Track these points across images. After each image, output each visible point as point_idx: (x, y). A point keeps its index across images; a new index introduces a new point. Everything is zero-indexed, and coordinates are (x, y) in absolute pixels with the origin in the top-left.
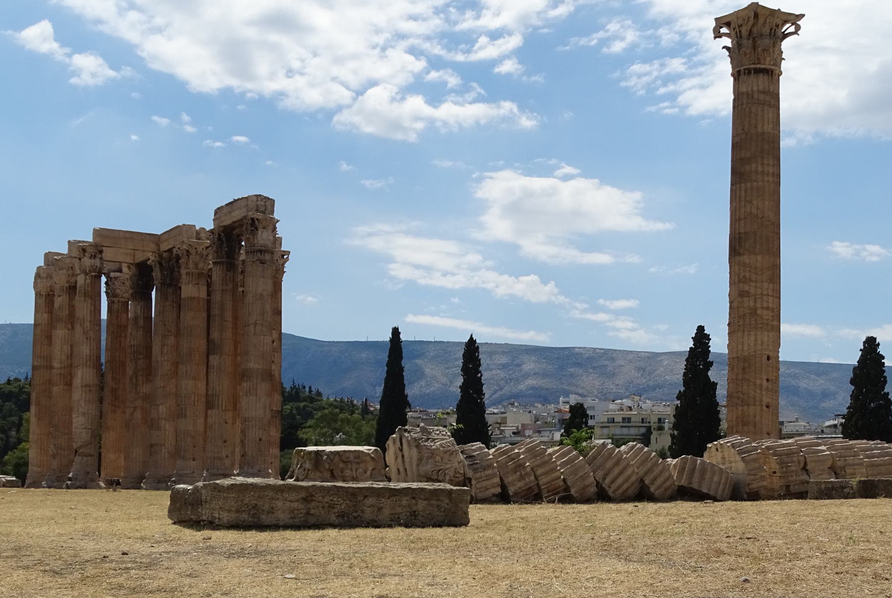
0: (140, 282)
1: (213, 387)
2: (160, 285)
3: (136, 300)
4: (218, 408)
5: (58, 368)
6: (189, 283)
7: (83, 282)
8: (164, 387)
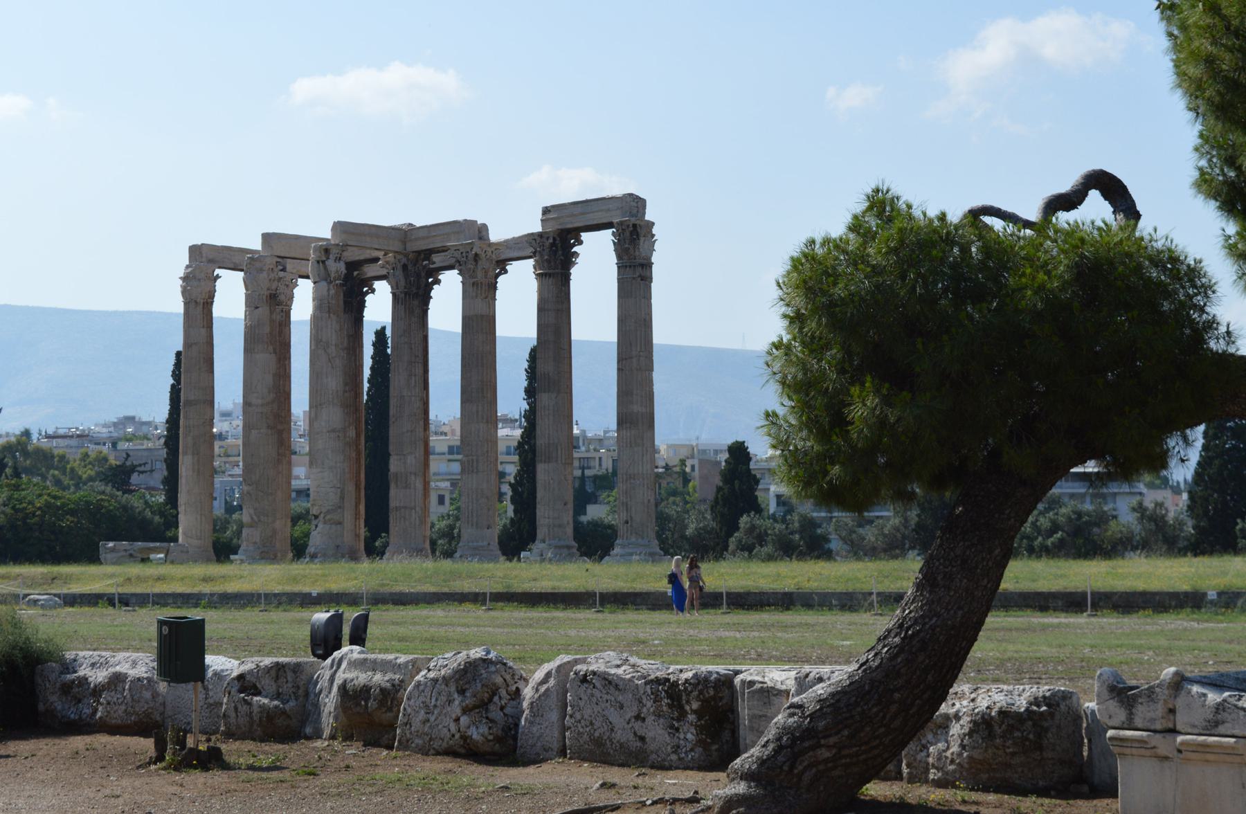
1: (549, 434)
4: (557, 461)
6: (476, 297)
7: (325, 293)
8: (412, 431)
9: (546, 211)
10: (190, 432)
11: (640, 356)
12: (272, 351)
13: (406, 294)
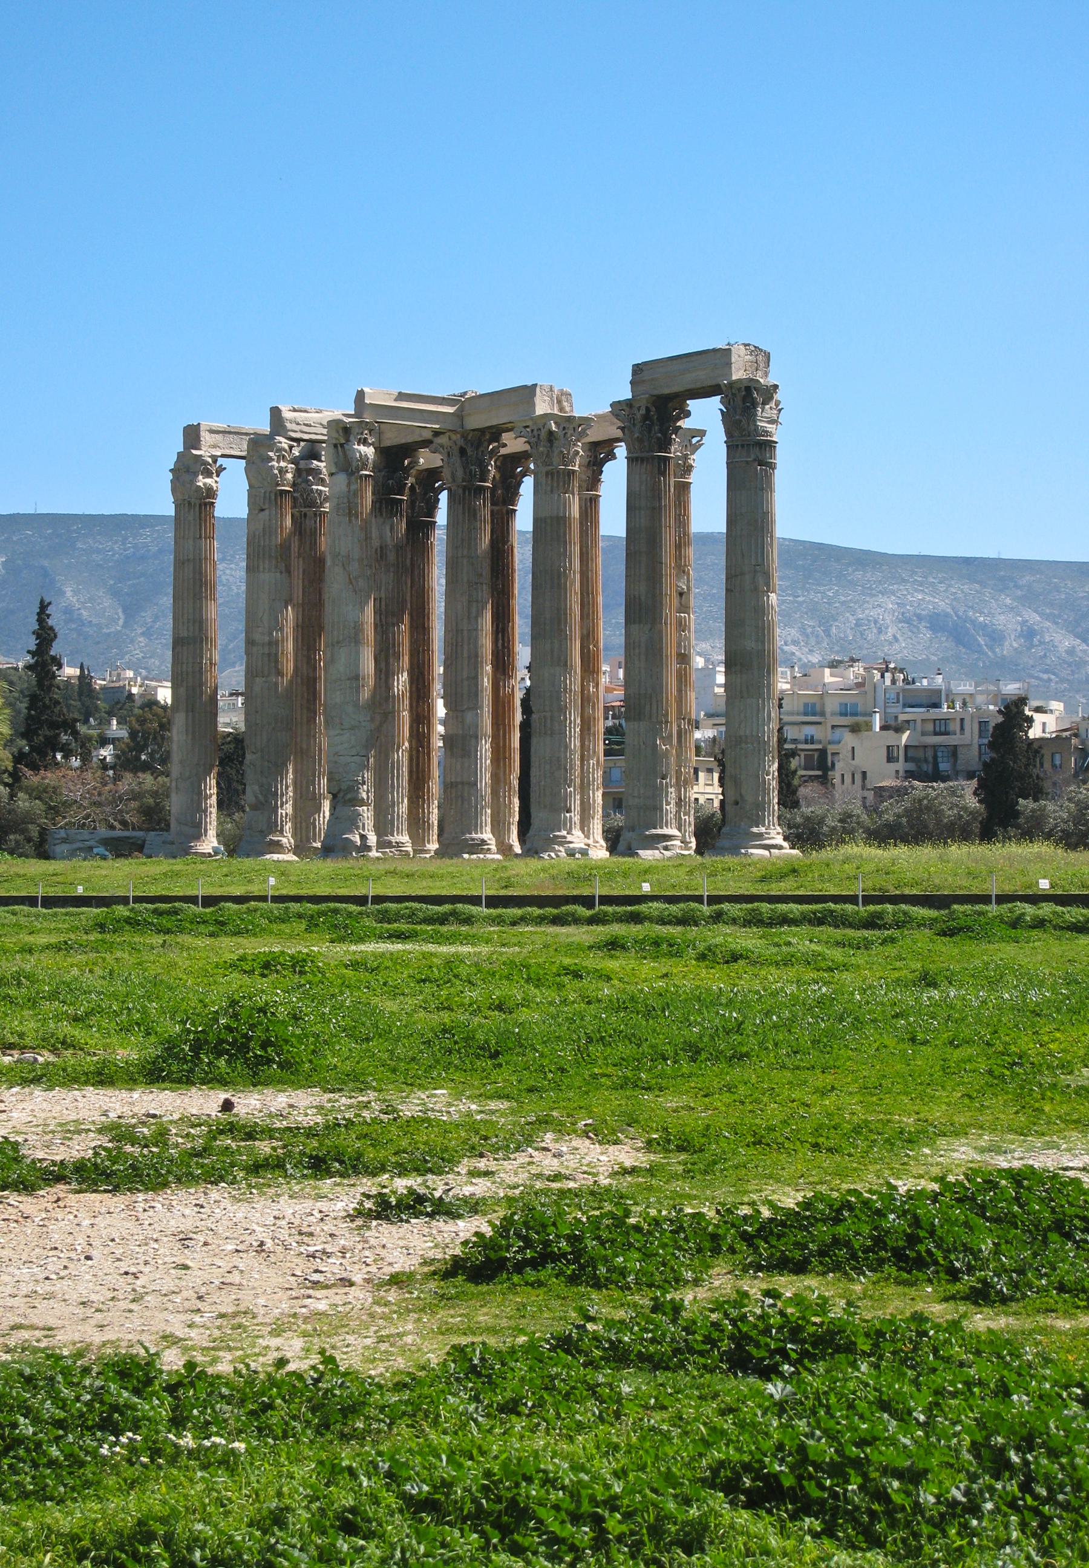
0: (390, 482)
2: (460, 491)
3: (381, 515)
4: (650, 718)
5: (263, 645)
6: (552, 491)
7: (344, 488)
9: (637, 369)
10: (182, 681)
11: (755, 571)
12: (284, 569)
13: (464, 488)
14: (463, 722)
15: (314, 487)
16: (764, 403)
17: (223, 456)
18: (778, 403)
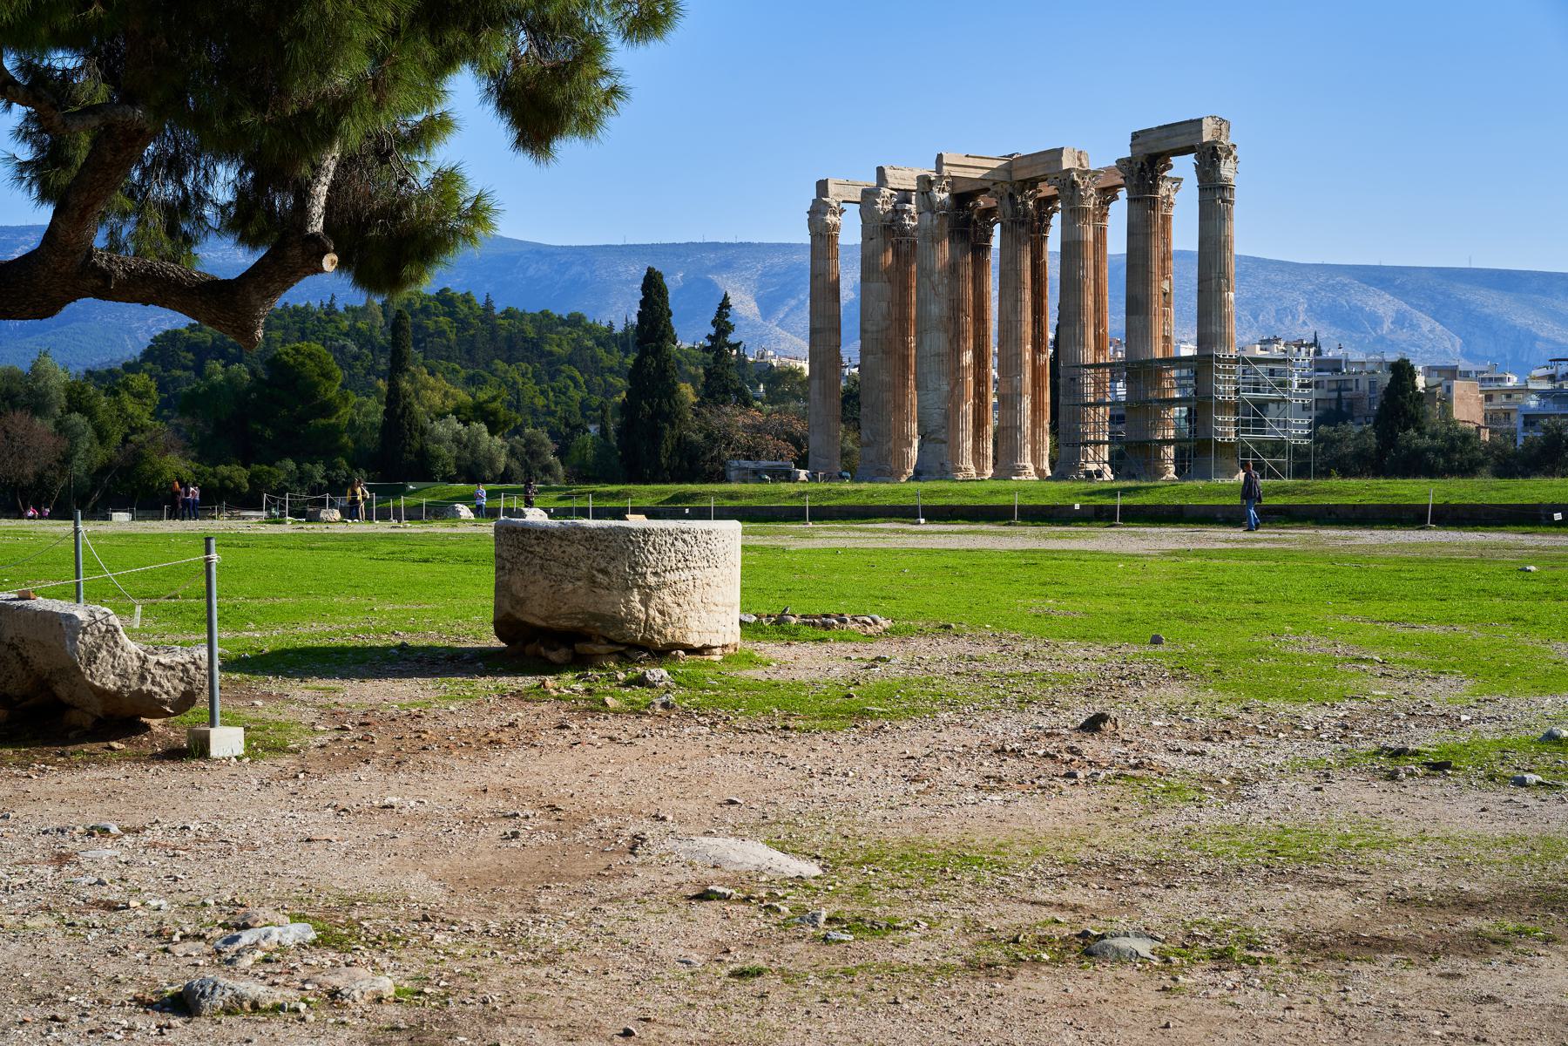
5: (872, 332)
7: (929, 223)
9: (1135, 136)
13: (1012, 222)
14: (1012, 385)
15: (907, 222)
16: (1226, 158)
17: (844, 202)
18: (1235, 158)
